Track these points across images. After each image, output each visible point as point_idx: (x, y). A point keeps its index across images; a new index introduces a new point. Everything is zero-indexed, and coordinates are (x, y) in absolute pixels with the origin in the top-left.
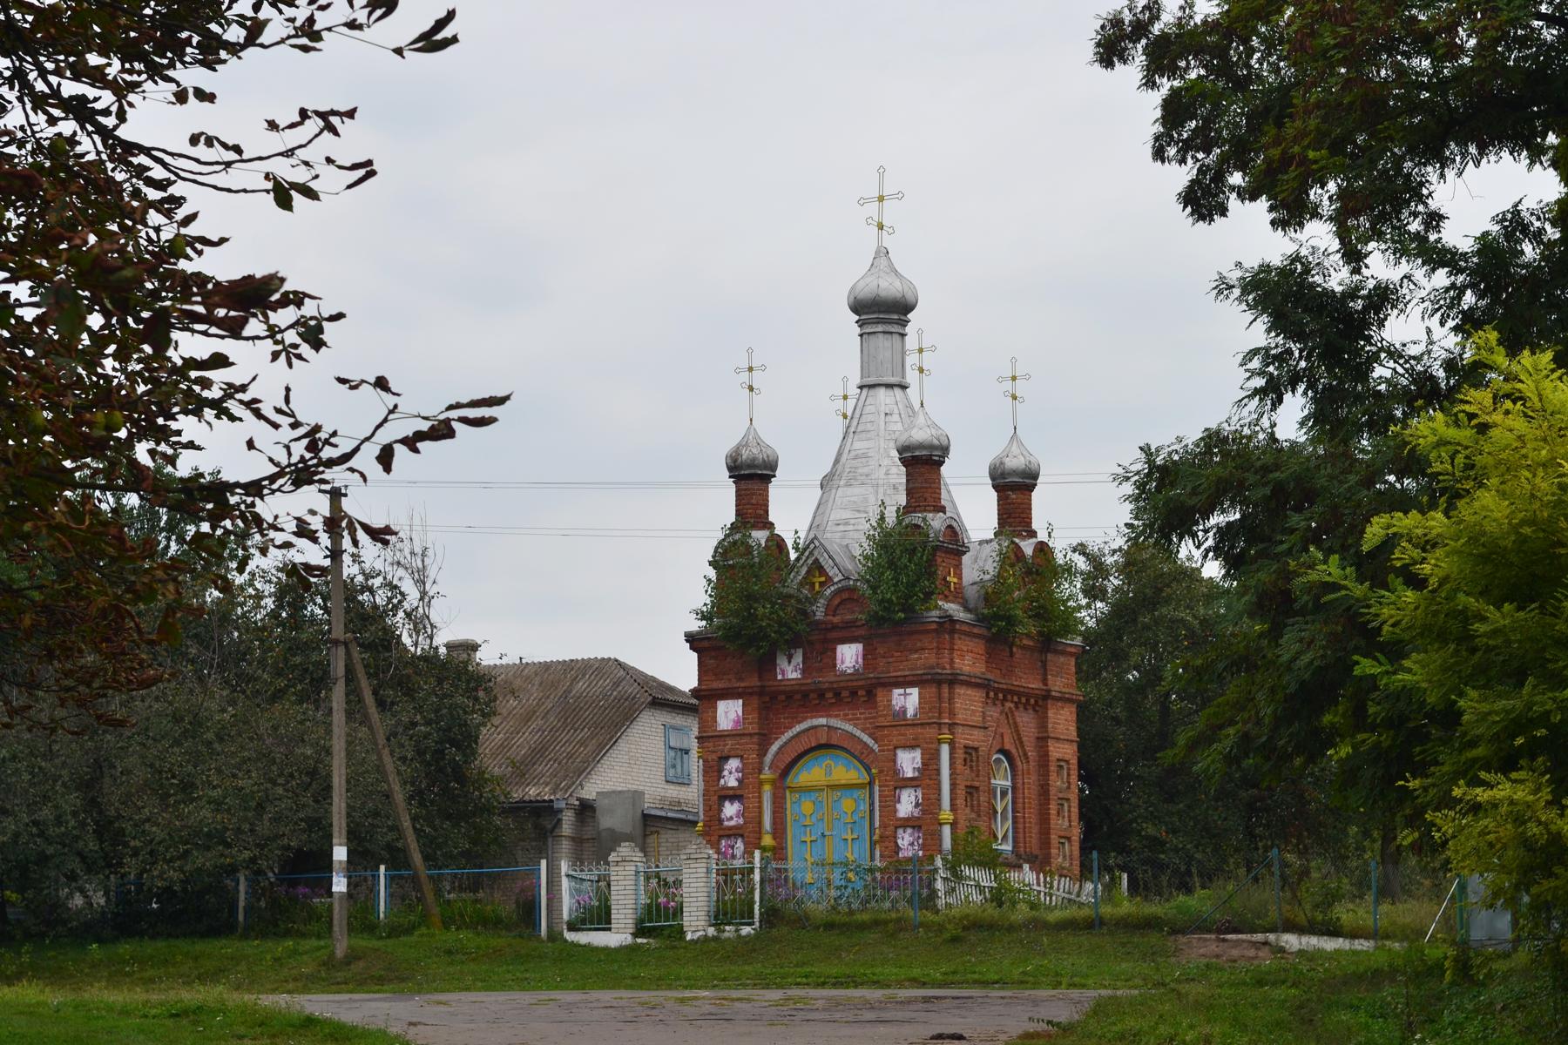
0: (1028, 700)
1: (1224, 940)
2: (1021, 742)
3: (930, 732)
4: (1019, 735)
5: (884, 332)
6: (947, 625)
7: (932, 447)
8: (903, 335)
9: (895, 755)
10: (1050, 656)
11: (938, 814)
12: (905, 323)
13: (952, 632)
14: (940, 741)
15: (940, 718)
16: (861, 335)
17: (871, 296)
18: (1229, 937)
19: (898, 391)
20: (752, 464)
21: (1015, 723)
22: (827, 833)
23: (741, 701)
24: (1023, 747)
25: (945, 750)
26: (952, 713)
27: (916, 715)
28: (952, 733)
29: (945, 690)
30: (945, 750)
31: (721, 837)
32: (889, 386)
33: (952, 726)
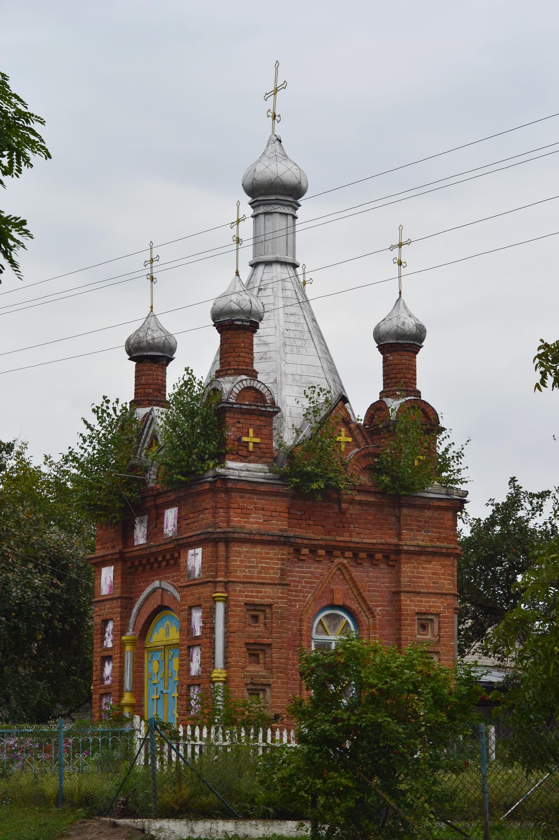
0: (164, 557)
1: (115, 825)
2: (363, 598)
3: (206, 590)
4: (358, 590)
5: (266, 213)
6: (219, 484)
7: (250, 313)
8: (295, 218)
9: (190, 614)
10: (405, 511)
11: (211, 673)
12: (297, 206)
13: (228, 491)
14: (215, 600)
15: (216, 576)
16: (255, 216)
17: (268, 178)
18: (121, 821)
19: (290, 270)
20: (152, 347)
21: (352, 579)
22: (165, 691)
23: (113, 567)
24: (365, 602)
25: (220, 608)
26: (228, 572)
27: (199, 575)
28: (227, 591)
29: (222, 548)
30: (220, 608)
31: (102, 695)
32: (283, 263)
33: (226, 584)
